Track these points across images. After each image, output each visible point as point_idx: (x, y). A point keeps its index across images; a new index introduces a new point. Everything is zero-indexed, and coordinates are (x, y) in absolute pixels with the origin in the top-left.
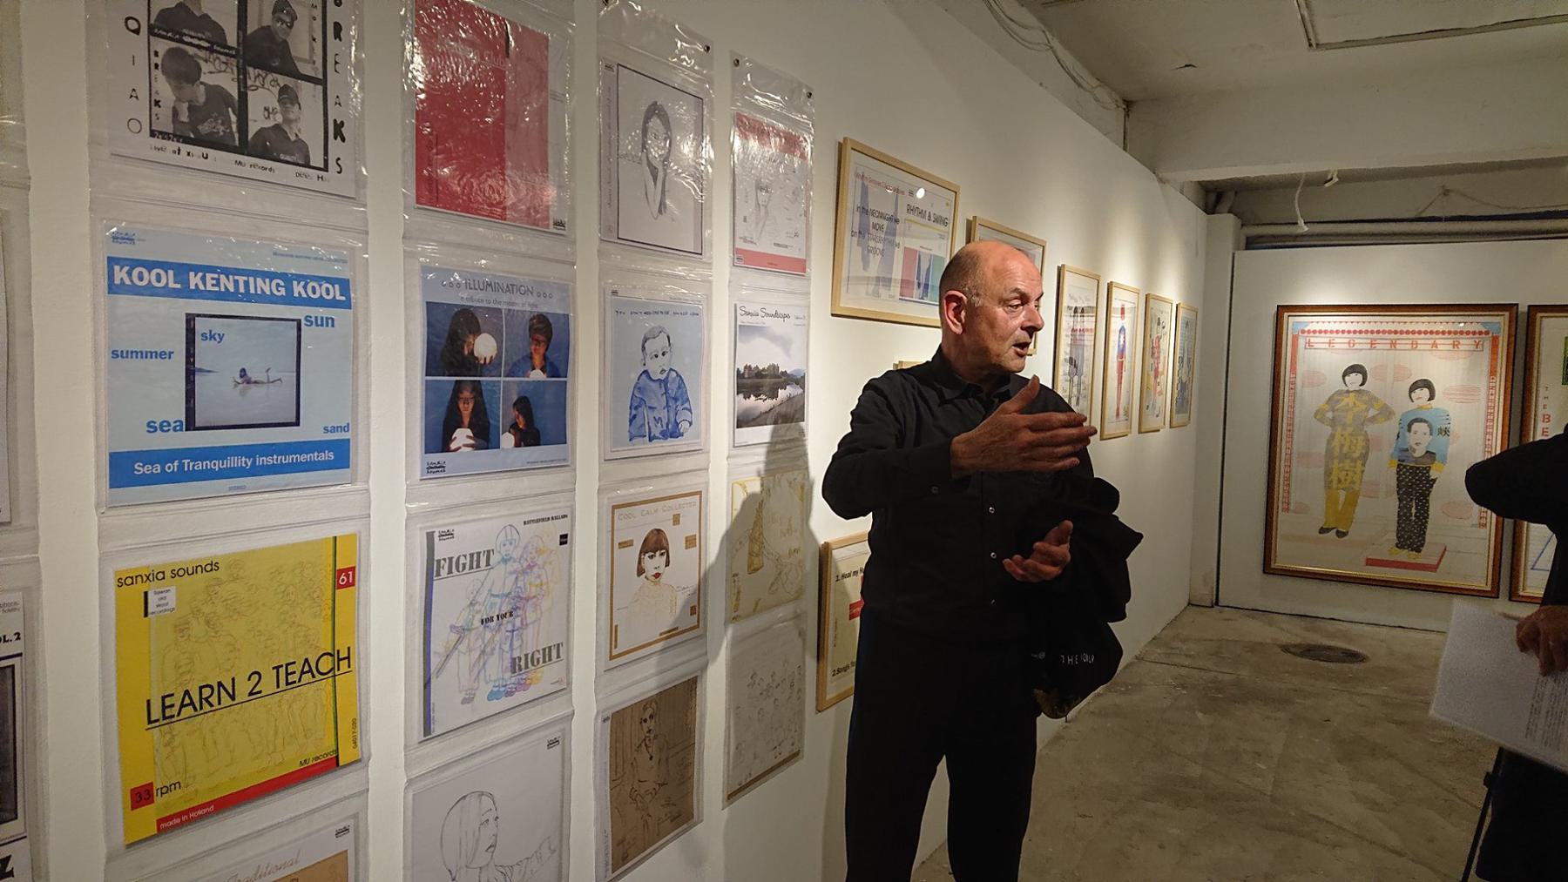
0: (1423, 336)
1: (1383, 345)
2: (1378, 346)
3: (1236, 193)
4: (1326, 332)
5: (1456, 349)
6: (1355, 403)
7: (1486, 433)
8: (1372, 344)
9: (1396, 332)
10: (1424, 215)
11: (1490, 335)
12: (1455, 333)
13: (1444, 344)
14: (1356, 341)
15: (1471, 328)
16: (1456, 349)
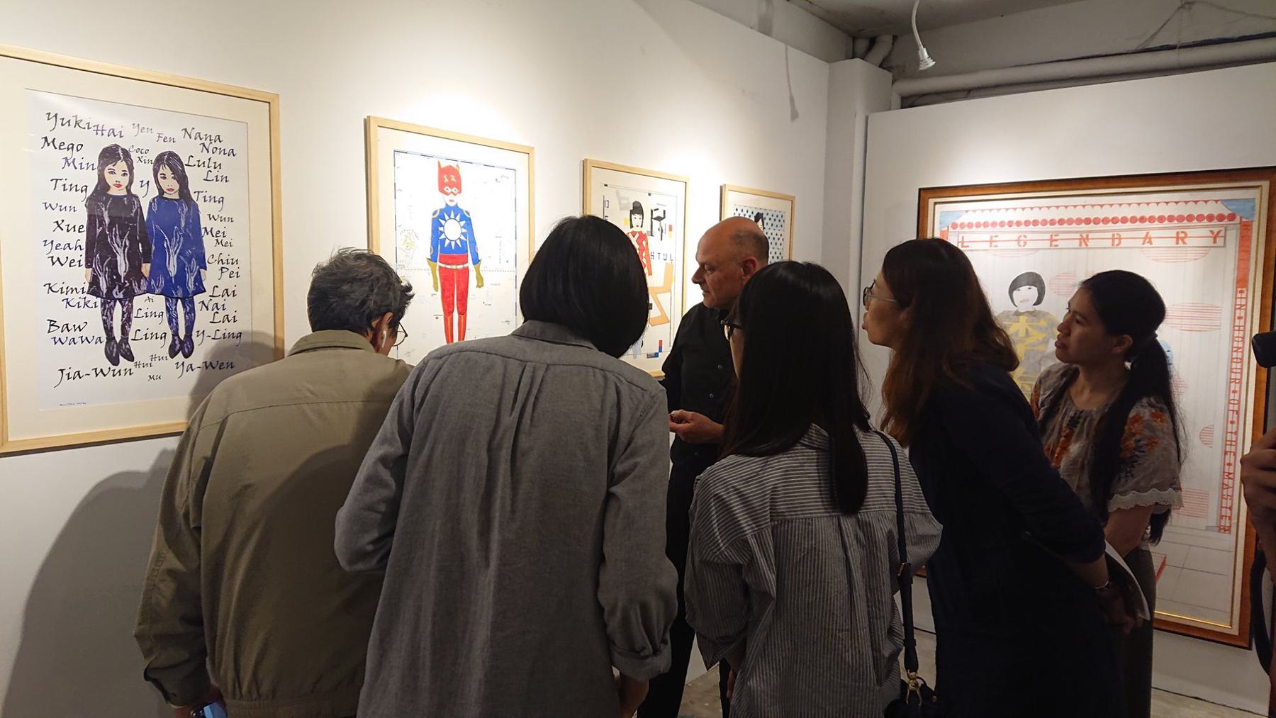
0: (1129, 225)
1: (1068, 241)
2: (1061, 244)
3: (895, 38)
4: (986, 225)
5: (1181, 243)
6: (1027, 331)
7: (1231, 381)
8: (1052, 240)
9: (1088, 221)
10: (1153, 45)
11: (1237, 220)
12: (1180, 219)
13: (1163, 236)
14: (1030, 236)
15: (1205, 210)
16: (1181, 243)
